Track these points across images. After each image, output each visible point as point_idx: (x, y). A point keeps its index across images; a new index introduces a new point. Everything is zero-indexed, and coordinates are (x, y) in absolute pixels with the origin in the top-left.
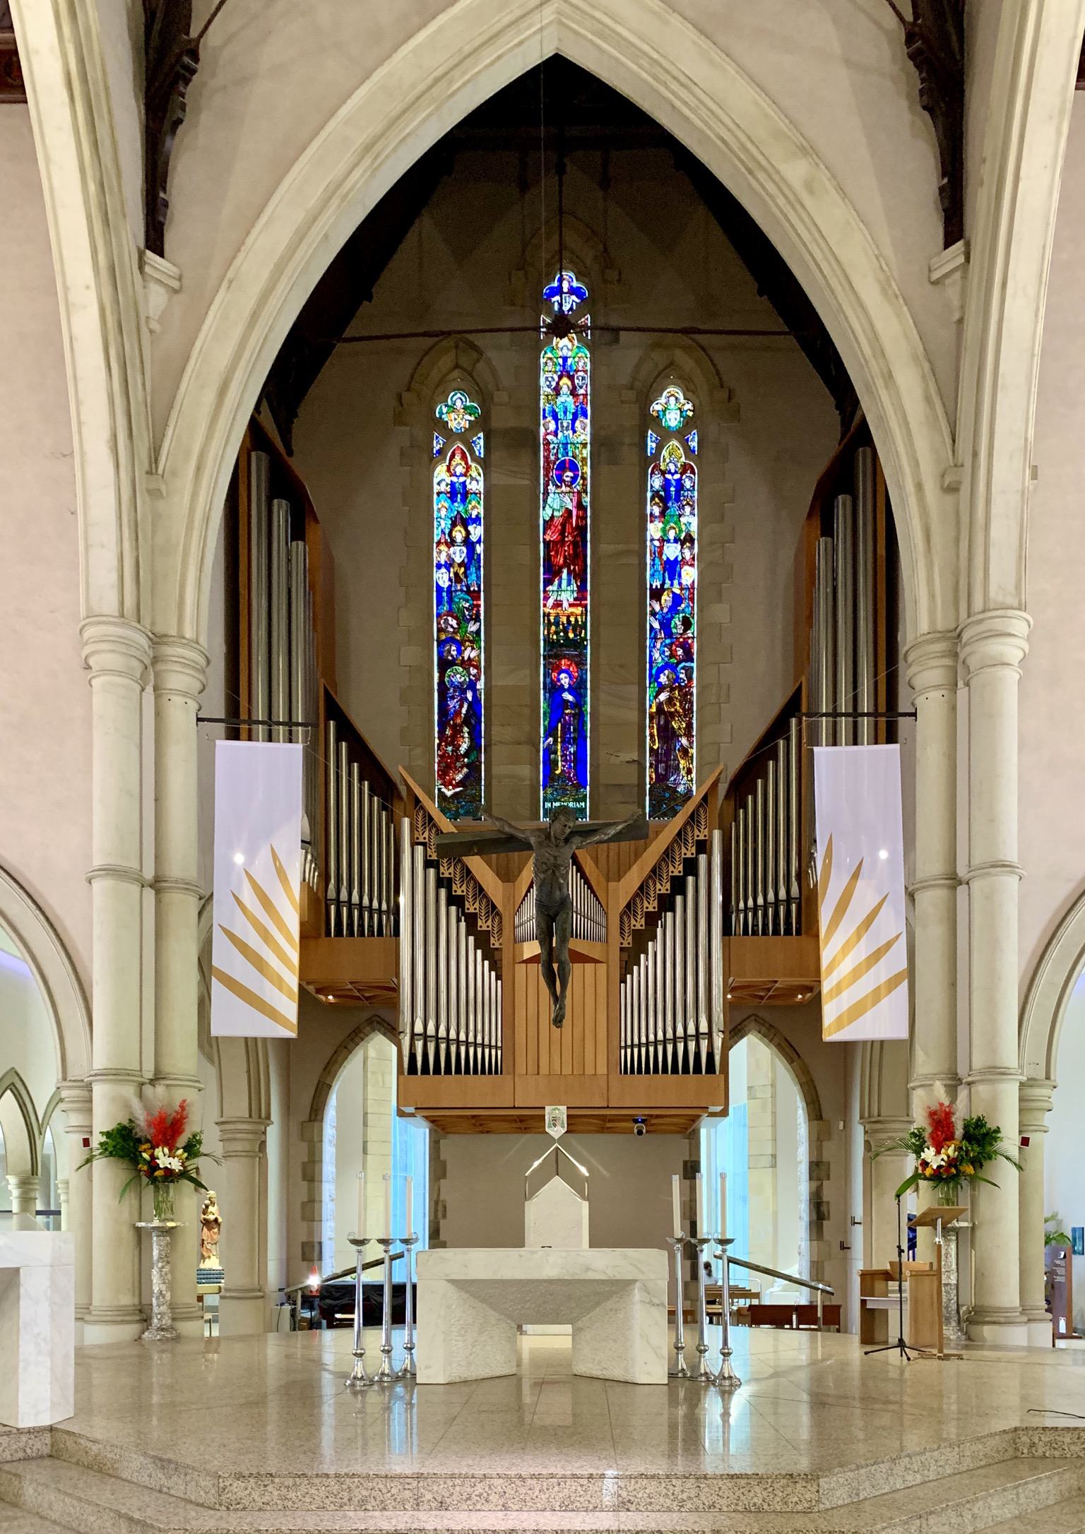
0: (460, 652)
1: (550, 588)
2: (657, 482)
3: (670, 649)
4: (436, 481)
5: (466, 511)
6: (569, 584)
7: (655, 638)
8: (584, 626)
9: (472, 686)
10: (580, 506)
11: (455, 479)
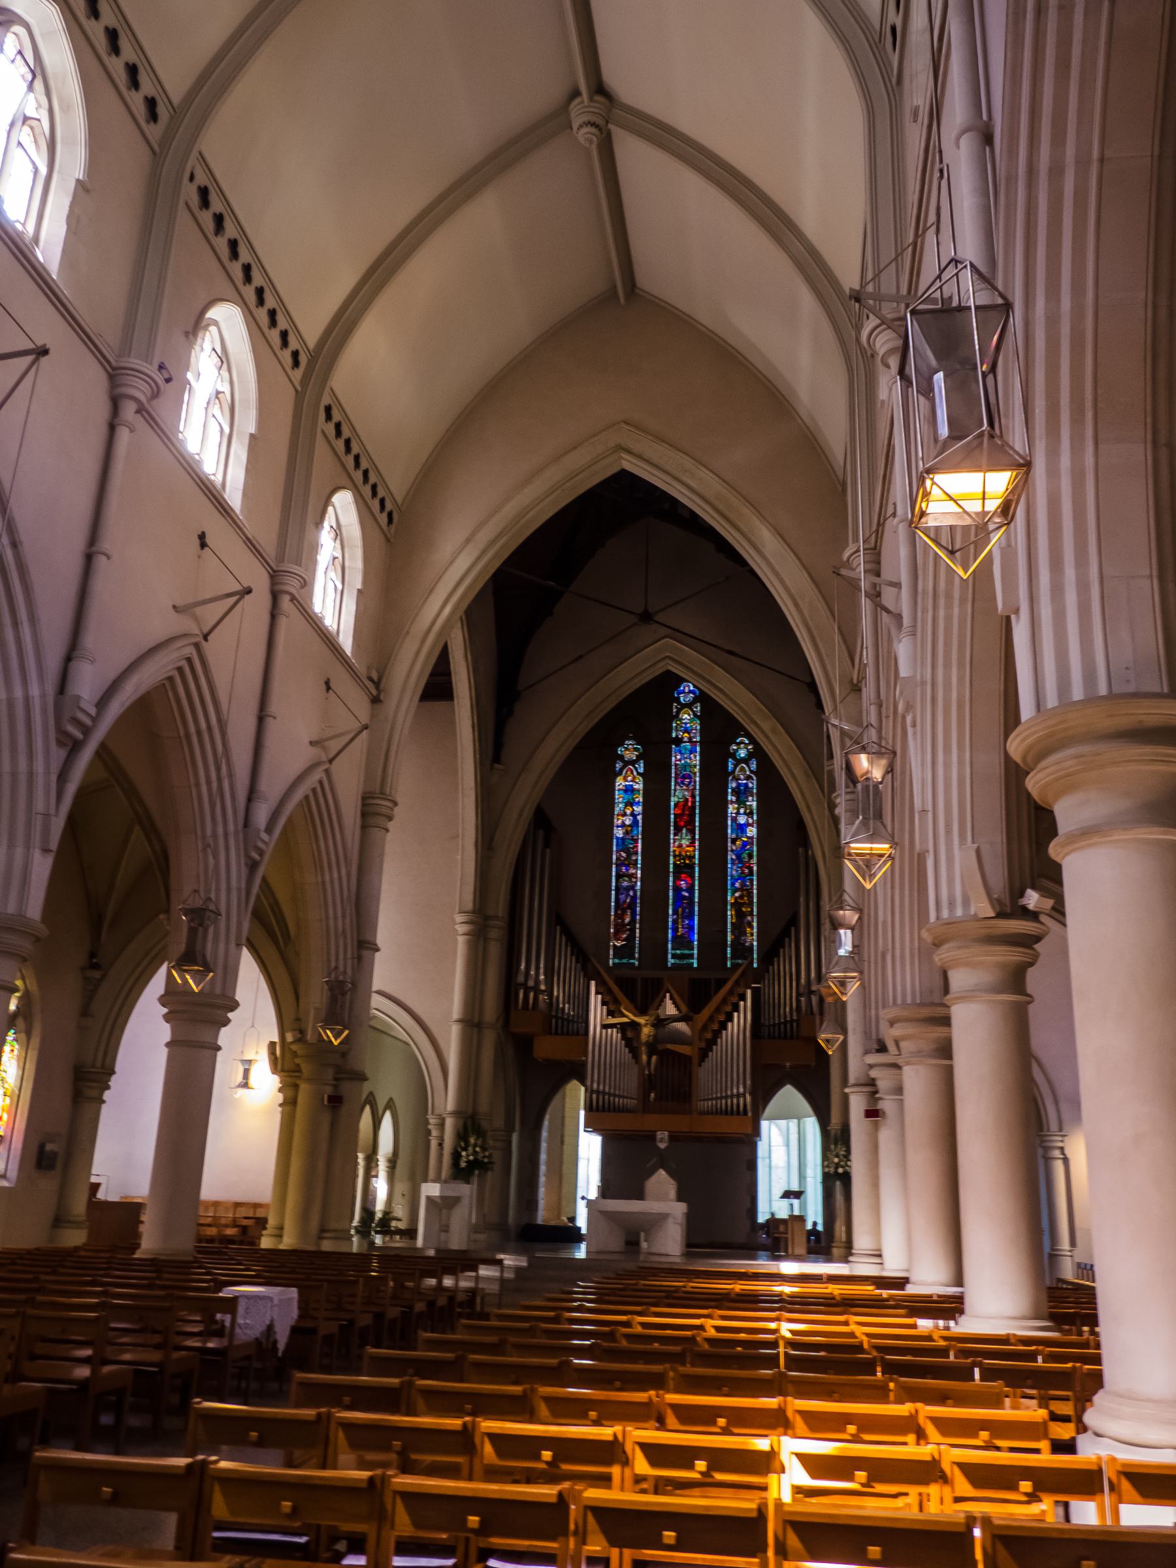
0: (627, 870)
2: (734, 785)
3: (742, 870)
4: (617, 784)
5: (634, 799)
6: (686, 835)
7: (733, 864)
8: (694, 857)
9: (633, 888)
11: (627, 783)
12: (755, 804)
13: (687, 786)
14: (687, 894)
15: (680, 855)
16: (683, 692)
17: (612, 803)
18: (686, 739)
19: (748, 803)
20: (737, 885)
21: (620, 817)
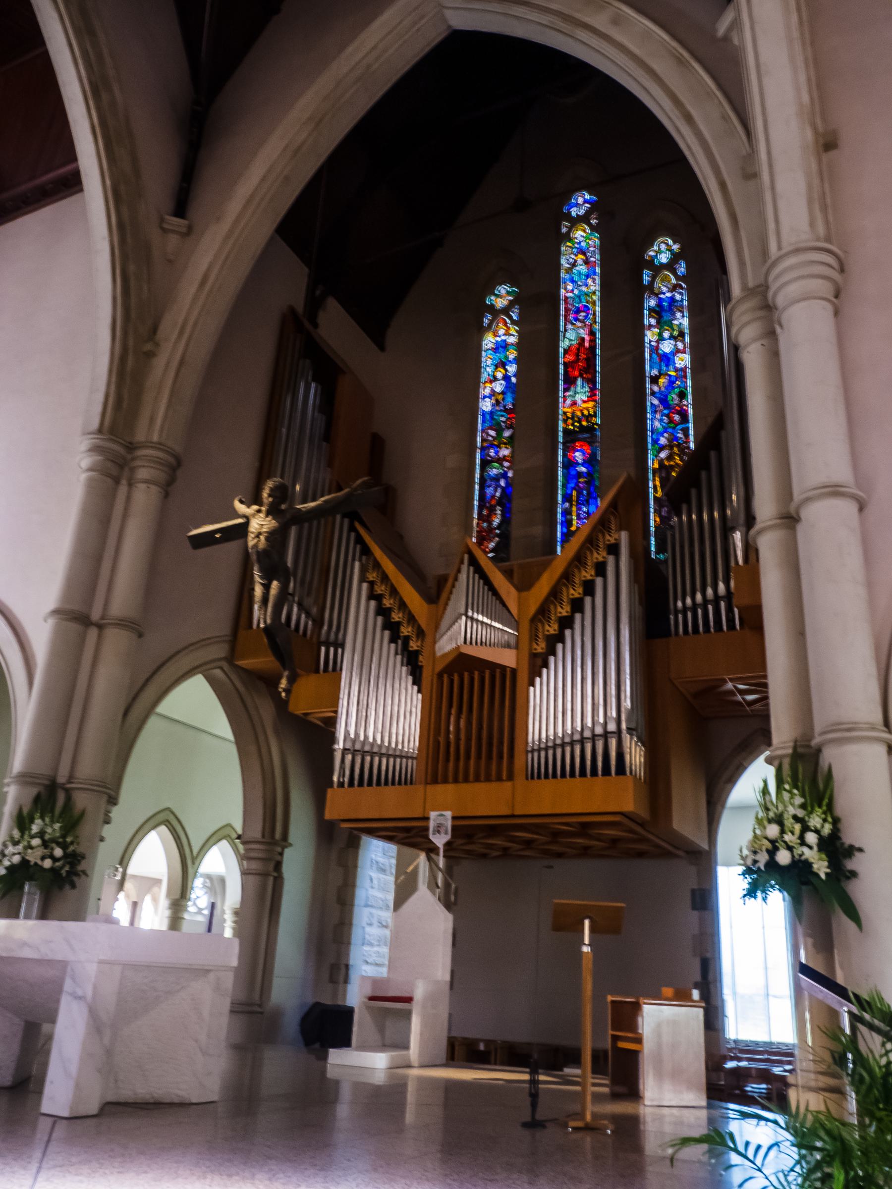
1: (568, 394)
2: (653, 303)
5: (507, 357)
6: (583, 387)
9: (504, 475)
10: (592, 334)
11: (498, 339)
12: (685, 322)
13: (582, 322)
14: (584, 469)
15: (572, 418)
16: (577, 205)
17: (478, 367)
18: (580, 262)
19: (675, 322)
20: (663, 441)
21: (488, 385)
